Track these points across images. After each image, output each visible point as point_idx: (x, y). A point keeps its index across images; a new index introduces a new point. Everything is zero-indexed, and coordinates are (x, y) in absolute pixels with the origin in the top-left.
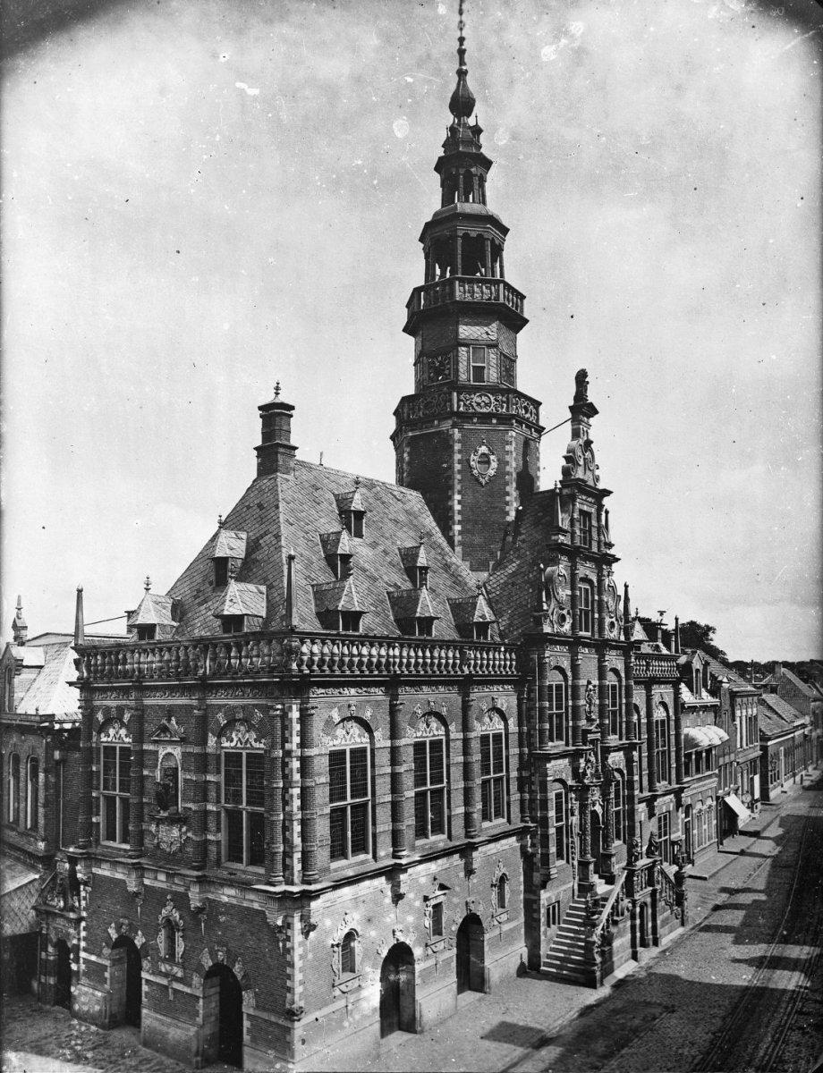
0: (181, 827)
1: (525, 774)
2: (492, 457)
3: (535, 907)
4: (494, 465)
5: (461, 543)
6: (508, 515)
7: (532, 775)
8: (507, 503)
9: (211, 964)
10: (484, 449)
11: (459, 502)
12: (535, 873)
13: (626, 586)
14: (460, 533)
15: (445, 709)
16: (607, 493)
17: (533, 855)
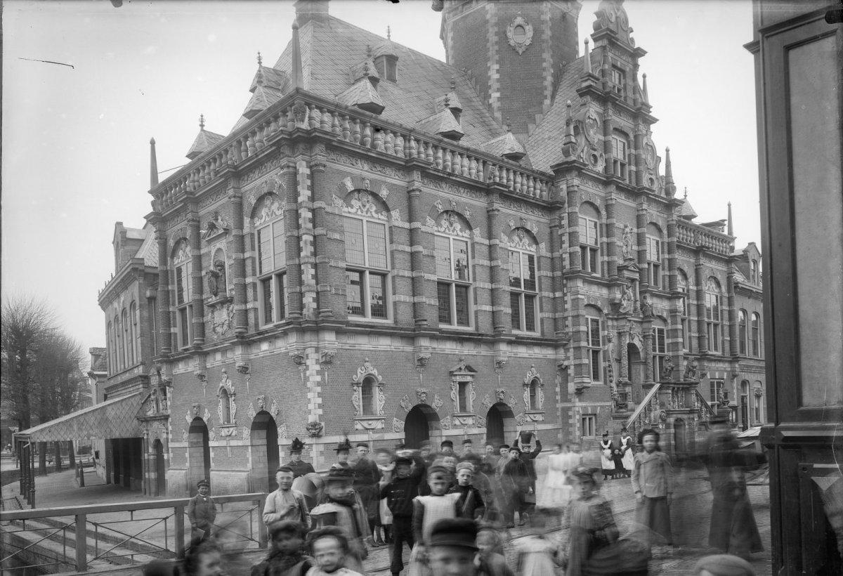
0: (229, 307)
1: (558, 294)
2: (527, 28)
3: (570, 413)
4: (530, 34)
5: (499, 109)
6: (545, 79)
7: (565, 295)
8: (544, 69)
9: (255, 414)
10: (519, 20)
11: (498, 71)
12: (569, 384)
13: (667, 151)
14: (499, 99)
15: (468, 213)
16: (639, 53)
17: (567, 367)
